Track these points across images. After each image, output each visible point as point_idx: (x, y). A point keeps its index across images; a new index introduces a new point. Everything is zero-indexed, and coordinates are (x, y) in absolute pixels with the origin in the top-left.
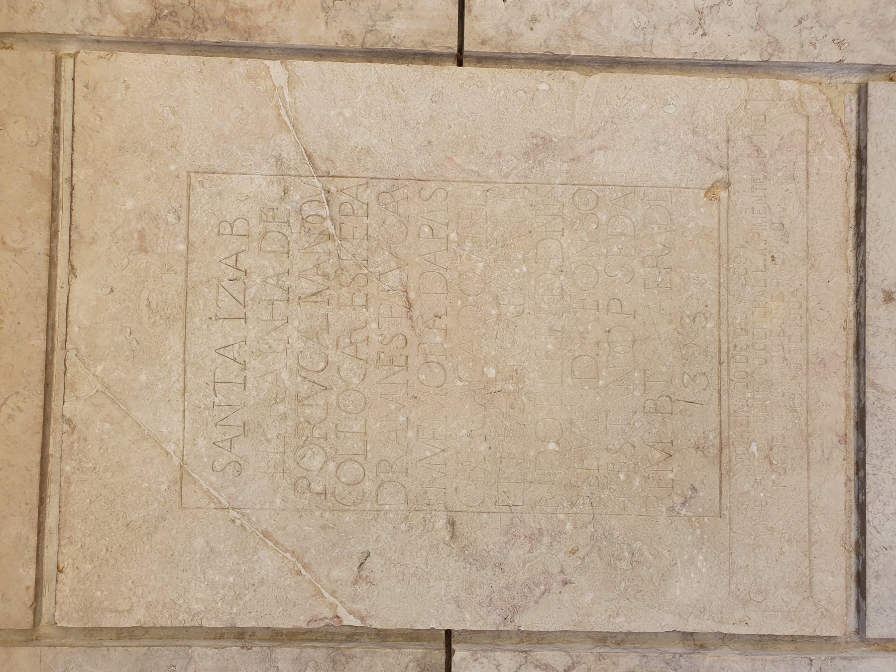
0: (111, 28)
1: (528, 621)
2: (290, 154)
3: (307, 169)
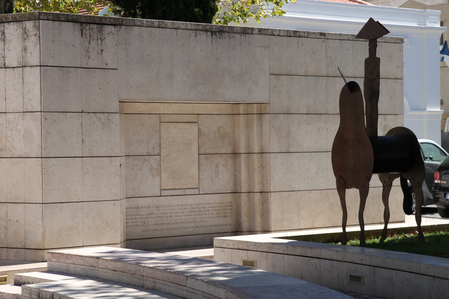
0: (199, 126)
1: (162, 161)
2: (192, 141)
3: (191, 142)
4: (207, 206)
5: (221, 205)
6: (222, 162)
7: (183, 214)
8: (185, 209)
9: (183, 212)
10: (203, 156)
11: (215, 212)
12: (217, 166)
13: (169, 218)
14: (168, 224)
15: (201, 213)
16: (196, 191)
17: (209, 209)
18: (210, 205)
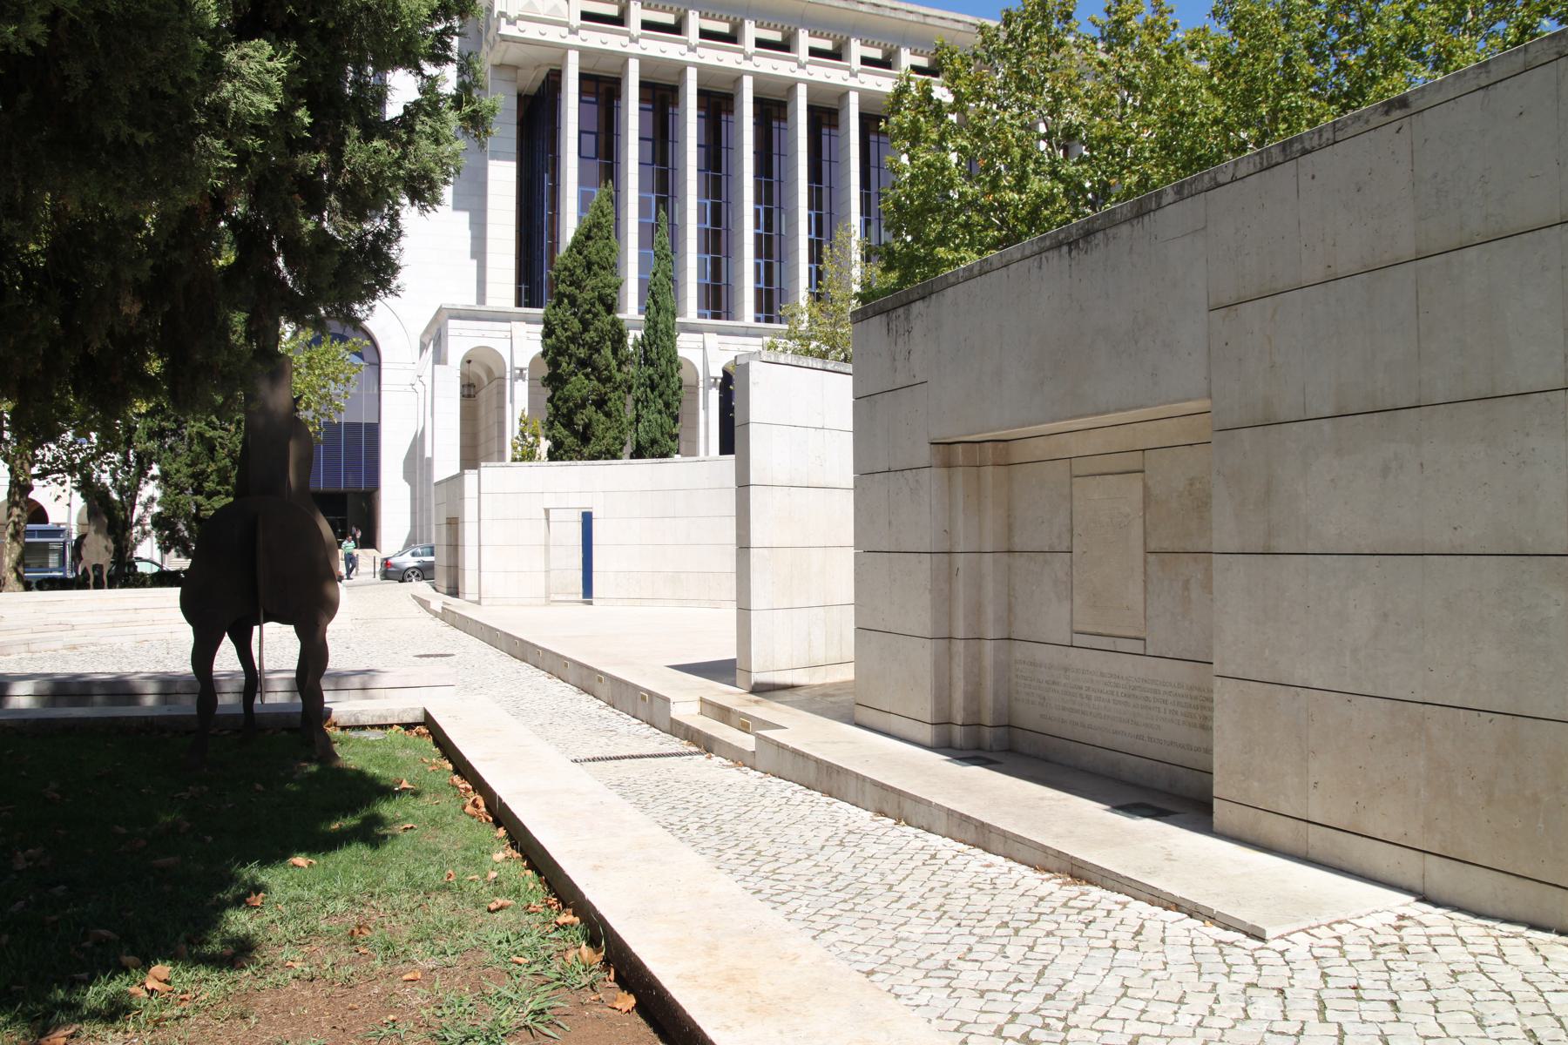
4: (1163, 689)
5: (1195, 693)
6: (1199, 576)
7: (1111, 697)
8: (1117, 686)
9: (1112, 693)
10: (1154, 556)
11: (1180, 710)
12: (1186, 585)
13: (1086, 701)
14: (1083, 713)
15: (1147, 703)
16: (1137, 646)
17: (1165, 697)
18: (1169, 689)
